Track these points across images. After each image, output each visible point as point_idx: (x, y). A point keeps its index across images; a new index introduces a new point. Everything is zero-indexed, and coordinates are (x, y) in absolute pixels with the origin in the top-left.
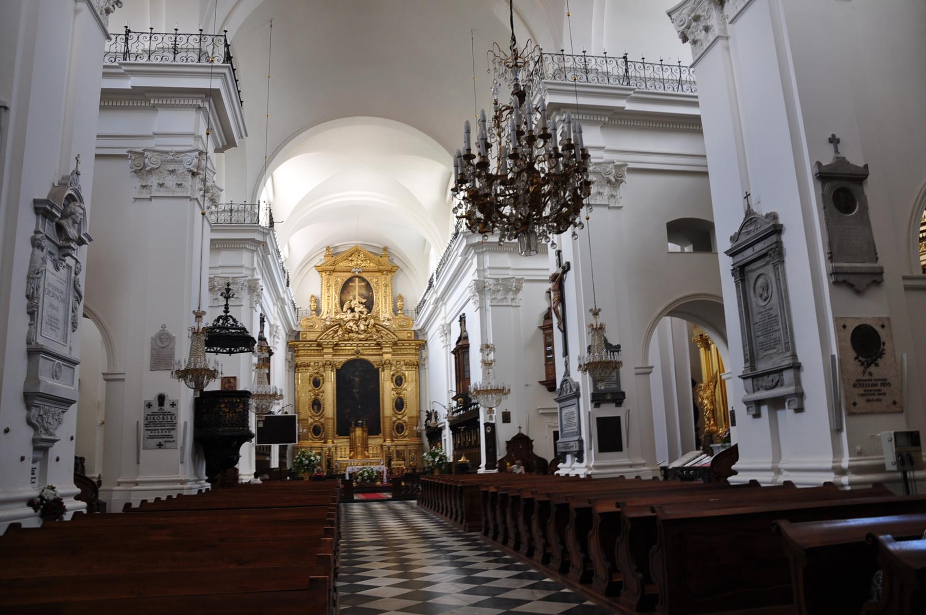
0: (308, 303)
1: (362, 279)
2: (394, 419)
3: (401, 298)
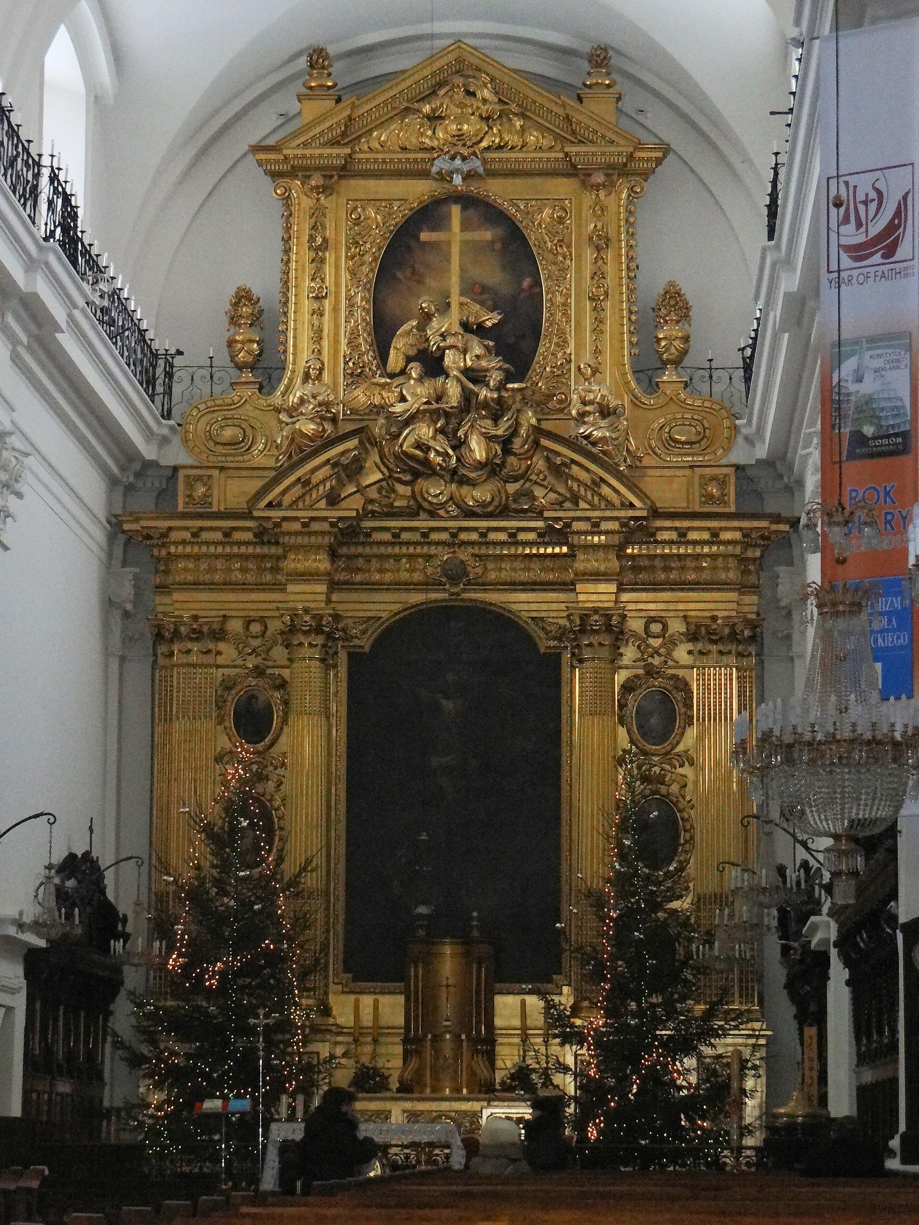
0: (221, 330)
3: (675, 303)
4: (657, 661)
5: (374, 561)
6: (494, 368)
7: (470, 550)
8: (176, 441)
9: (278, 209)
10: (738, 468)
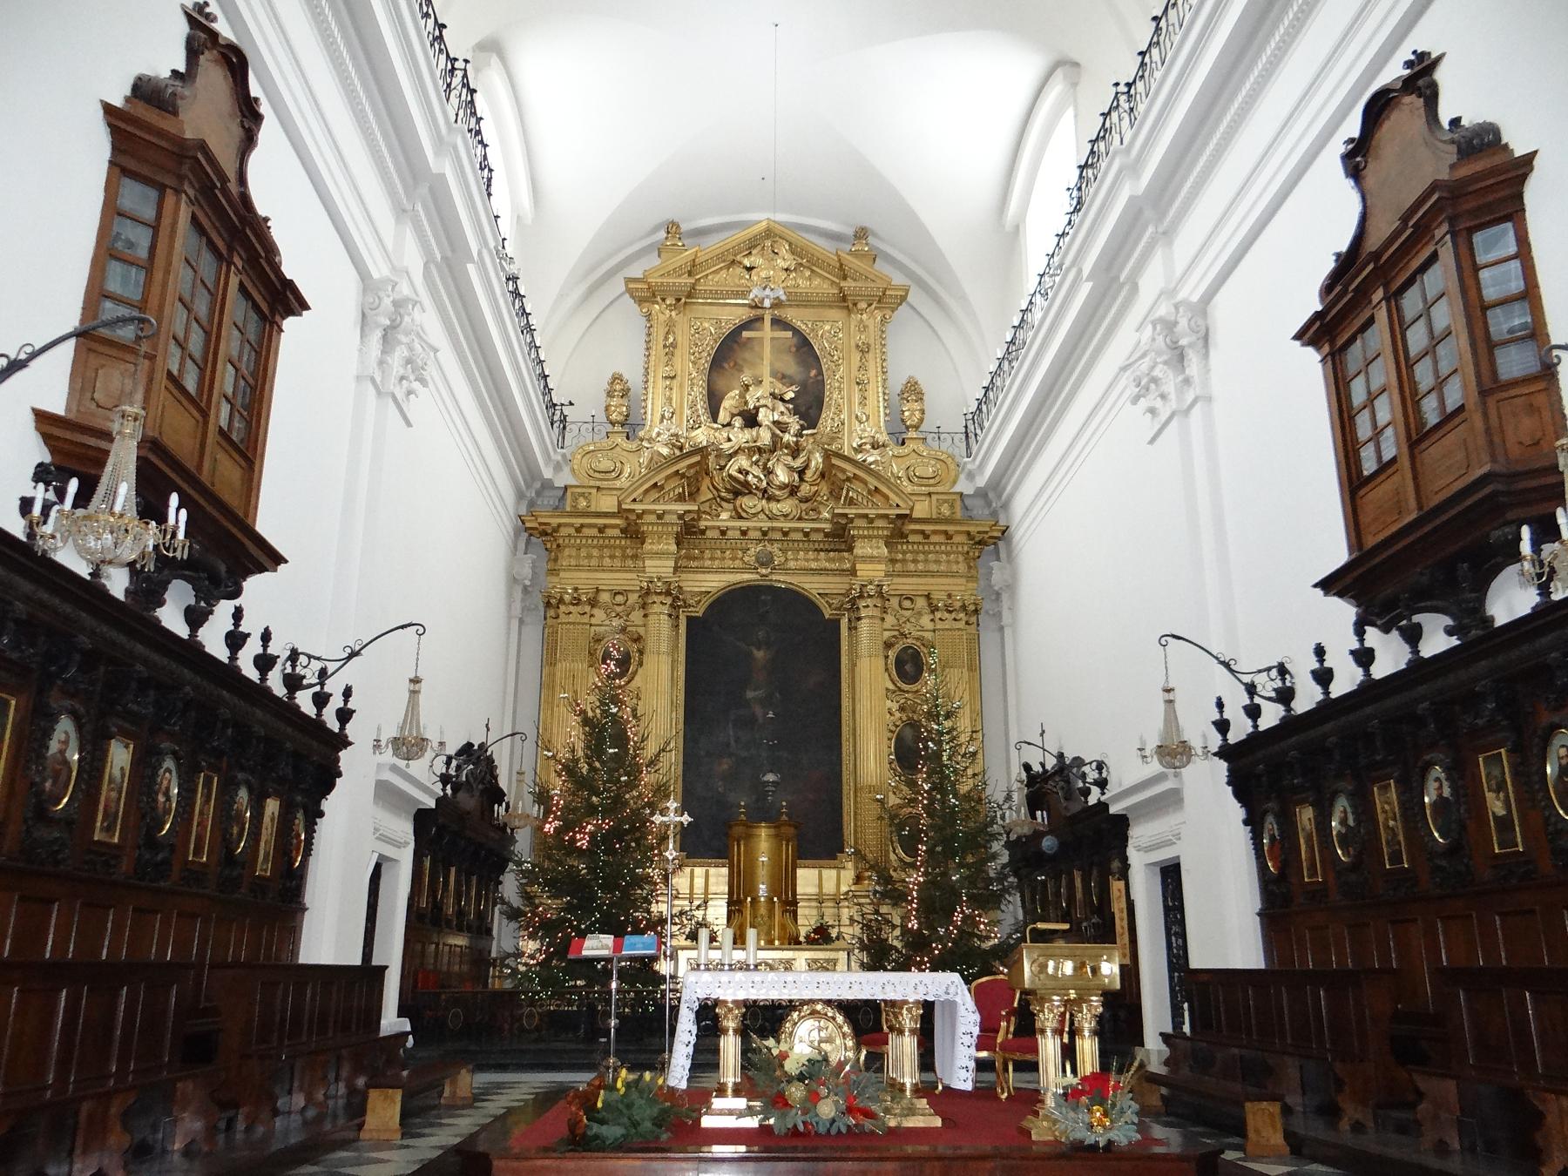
1: (778, 323)
3: (913, 390)
6: (794, 423)
8: (567, 469)
10: (961, 494)
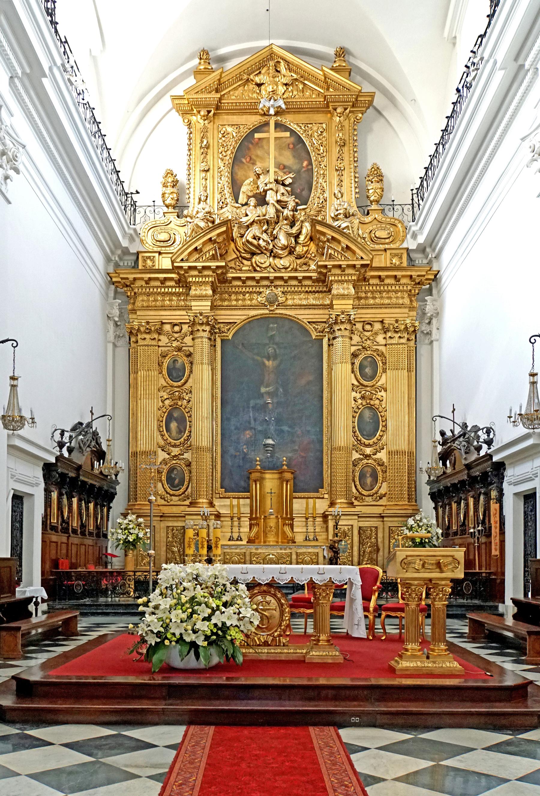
0: (160, 189)
2: (356, 456)
4: (369, 342)
5: (233, 295)
7: (279, 289)
9: (186, 130)
10: (407, 249)
